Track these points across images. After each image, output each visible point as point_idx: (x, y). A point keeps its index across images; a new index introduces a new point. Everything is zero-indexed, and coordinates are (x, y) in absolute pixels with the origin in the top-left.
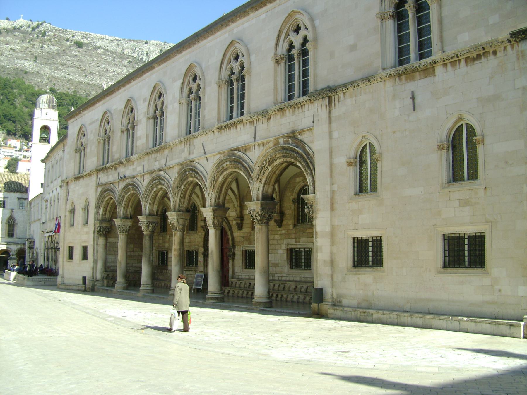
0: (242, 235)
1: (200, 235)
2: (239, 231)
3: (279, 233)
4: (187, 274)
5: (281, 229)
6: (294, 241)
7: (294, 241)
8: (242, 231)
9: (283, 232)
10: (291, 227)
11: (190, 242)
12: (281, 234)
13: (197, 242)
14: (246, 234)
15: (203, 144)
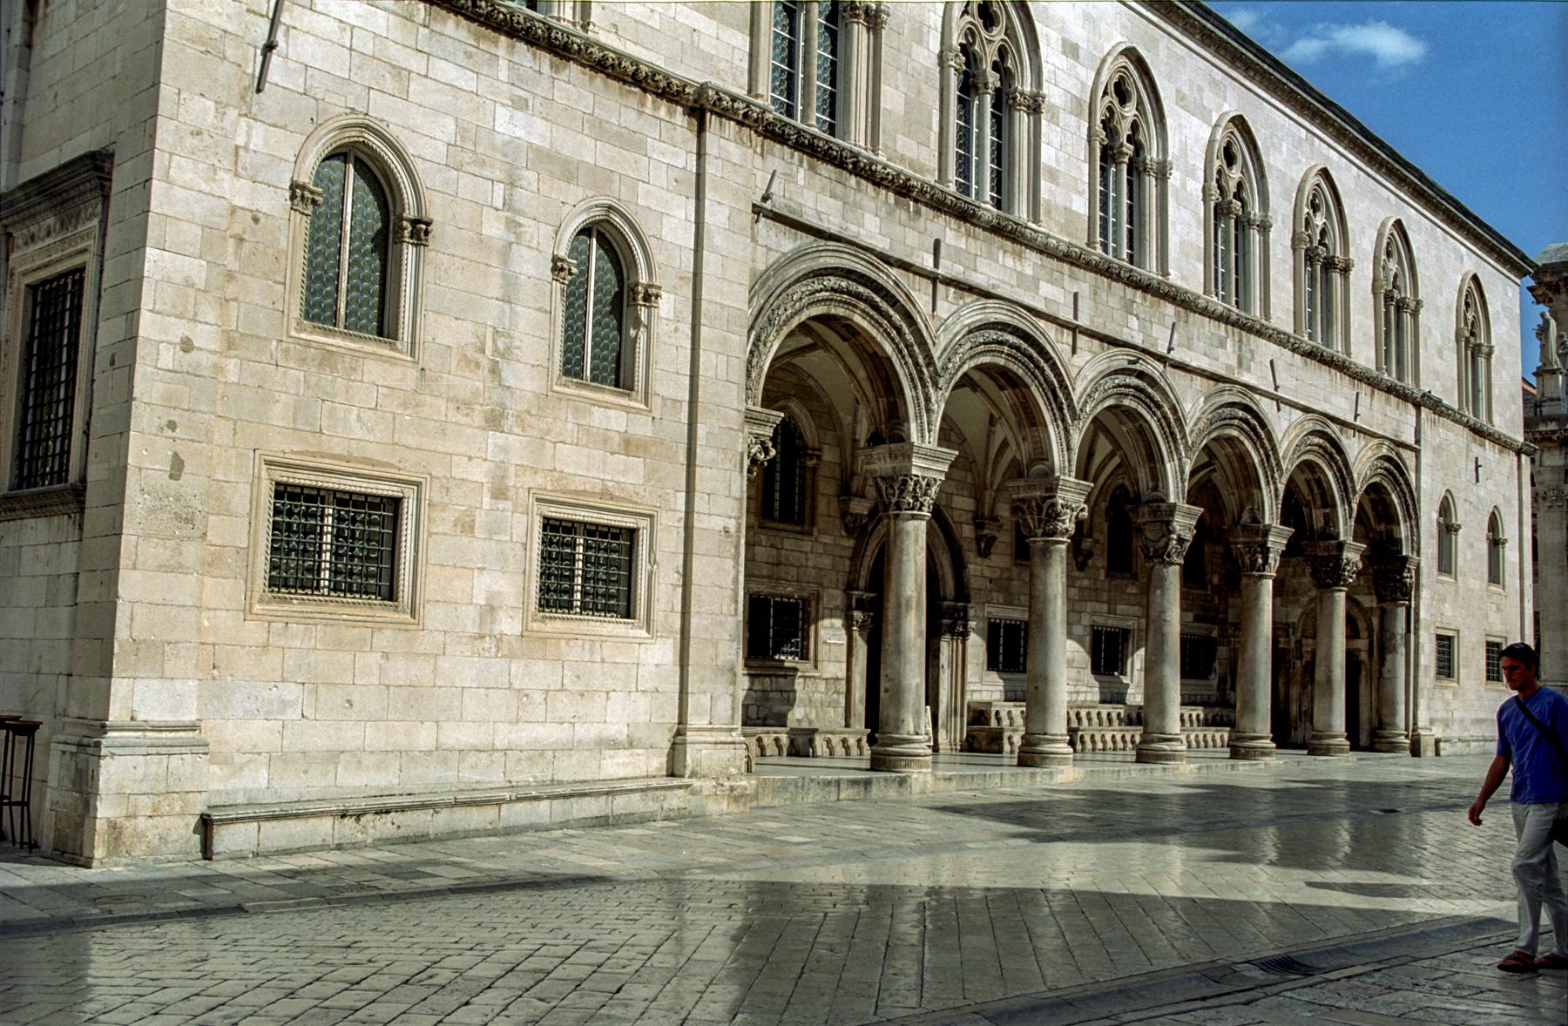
0: (987, 573)
1: (825, 544)
2: (979, 560)
3: (1078, 583)
4: (763, 691)
5: (1082, 574)
6: (1105, 607)
7: (1105, 607)
8: (987, 562)
9: (1086, 583)
10: (1102, 577)
11: (778, 564)
12: (1081, 589)
13: (814, 567)
14: (998, 572)
15: (1272, 362)
